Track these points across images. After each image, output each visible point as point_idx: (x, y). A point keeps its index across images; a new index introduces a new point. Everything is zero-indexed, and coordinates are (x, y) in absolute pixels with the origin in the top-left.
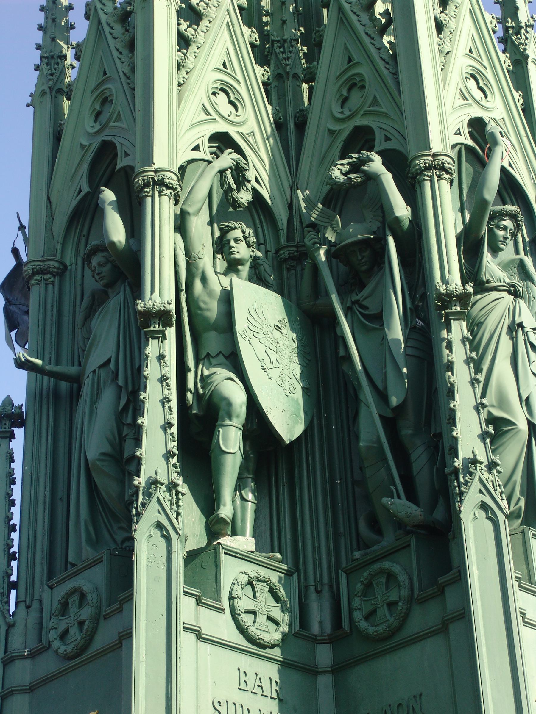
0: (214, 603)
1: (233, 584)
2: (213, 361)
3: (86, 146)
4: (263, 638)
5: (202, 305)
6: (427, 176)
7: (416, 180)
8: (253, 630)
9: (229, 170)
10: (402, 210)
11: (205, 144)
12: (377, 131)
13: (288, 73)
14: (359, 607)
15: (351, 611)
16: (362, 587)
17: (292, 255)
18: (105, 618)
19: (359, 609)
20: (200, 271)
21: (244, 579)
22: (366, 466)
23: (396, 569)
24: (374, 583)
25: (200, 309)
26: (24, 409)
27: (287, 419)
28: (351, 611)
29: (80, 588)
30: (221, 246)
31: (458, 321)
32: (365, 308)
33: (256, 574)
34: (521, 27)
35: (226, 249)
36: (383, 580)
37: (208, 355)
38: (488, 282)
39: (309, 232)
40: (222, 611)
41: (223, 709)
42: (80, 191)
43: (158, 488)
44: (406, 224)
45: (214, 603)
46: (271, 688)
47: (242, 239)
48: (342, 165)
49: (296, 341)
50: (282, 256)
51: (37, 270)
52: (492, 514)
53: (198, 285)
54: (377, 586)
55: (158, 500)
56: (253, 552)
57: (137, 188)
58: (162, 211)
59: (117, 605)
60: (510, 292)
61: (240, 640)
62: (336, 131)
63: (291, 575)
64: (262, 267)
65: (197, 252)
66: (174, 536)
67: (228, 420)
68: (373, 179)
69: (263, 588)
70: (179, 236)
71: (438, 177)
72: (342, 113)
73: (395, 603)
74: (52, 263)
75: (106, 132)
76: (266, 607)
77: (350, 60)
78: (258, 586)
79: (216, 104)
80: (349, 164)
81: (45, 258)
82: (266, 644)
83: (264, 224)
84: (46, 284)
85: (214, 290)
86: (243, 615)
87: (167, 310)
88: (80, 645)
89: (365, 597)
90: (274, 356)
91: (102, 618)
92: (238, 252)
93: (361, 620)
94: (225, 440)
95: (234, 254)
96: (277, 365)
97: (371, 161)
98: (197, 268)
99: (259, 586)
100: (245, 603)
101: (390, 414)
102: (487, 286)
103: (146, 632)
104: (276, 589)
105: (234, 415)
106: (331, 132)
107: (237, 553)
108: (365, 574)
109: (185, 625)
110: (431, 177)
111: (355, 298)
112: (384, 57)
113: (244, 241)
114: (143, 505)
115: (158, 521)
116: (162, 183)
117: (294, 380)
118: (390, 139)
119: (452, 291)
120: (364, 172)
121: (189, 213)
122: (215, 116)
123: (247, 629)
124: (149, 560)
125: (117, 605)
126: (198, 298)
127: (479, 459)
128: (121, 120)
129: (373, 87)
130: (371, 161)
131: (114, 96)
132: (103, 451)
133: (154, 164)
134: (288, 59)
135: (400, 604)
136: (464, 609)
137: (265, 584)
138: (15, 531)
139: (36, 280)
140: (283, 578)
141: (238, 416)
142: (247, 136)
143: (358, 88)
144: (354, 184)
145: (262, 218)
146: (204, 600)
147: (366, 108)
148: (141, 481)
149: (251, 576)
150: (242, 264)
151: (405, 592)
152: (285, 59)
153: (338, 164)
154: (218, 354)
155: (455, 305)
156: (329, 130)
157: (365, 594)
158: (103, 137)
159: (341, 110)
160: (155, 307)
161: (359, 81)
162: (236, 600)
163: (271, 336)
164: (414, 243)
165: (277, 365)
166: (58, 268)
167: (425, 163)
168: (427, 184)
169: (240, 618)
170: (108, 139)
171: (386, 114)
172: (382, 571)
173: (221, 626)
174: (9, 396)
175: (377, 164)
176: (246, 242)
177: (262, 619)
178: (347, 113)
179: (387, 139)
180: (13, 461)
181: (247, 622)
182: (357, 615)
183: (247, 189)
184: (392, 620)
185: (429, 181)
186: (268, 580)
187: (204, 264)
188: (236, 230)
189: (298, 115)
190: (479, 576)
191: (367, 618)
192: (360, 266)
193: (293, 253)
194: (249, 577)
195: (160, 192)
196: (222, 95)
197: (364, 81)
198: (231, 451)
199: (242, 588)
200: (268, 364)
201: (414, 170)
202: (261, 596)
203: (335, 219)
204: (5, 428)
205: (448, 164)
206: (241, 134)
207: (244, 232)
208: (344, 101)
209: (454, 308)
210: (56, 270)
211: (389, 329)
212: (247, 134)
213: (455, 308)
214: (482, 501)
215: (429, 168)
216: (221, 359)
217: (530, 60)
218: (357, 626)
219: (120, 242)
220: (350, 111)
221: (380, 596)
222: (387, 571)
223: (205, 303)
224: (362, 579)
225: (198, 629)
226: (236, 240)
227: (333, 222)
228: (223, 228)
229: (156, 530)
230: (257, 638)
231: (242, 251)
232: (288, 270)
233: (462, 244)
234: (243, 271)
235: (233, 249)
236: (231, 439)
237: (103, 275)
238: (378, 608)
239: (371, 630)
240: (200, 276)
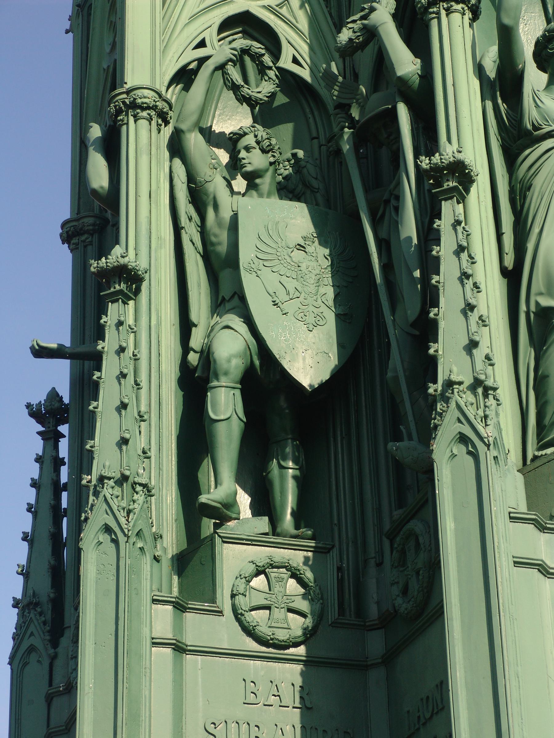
0: (206, 606)
4: (277, 637)
5: (213, 239)
6: (433, 13)
8: (264, 630)
9: (230, 63)
14: (396, 581)
20: (211, 197)
27: (310, 360)
31: (450, 201)
37: (223, 299)
38: (536, 128)
41: (219, 731)
43: (106, 484)
44: (416, 80)
45: (206, 606)
46: (291, 696)
47: (255, 145)
48: (354, 21)
49: (328, 257)
51: (73, 233)
52: (472, 447)
56: (266, 534)
61: (252, 645)
64: (305, 170)
65: (202, 175)
66: (122, 539)
67: (216, 381)
70: (177, 162)
74: (86, 220)
78: (273, 575)
81: (82, 214)
82: (283, 643)
83: (316, 113)
84: (85, 247)
87: (121, 265)
90: (291, 285)
92: (250, 163)
93: (398, 596)
94: (213, 407)
95: (245, 167)
96: (297, 294)
98: (206, 194)
102: (536, 136)
103: (95, 658)
104: (301, 574)
105: (220, 373)
107: (243, 539)
109: (154, 641)
110: (438, 13)
113: (258, 147)
116: (134, 105)
117: (324, 308)
119: (437, 164)
121: (182, 131)
123: (254, 630)
124: (99, 572)
126: (210, 231)
127: (453, 380)
133: (126, 83)
137: (284, 570)
139: (73, 244)
140: (311, 558)
141: (226, 374)
142: (277, 8)
144: (357, 45)
149: (259, 564)
150: (260, 176)
153: (348, 23)
154: (232, 297)
155: (448, 180)
162: (237, 597)
163: (289, 260)
165: (297, 294)
166: (94, 225)
169: (243, 618)
173: (221, 631)
174: (54, 388)
176: (260, 148)
181: (253, 622)
183: (270, 78)
185: (436, 20)
186: (287, 564)
187: (215, 187)
188: (247, 136)
190: (457, 530)
195: (135, 116)
198: (222, 417)
203: (359, 92)
204: (49, 427)
207: (256, 136)
210: (91, 228)
211: (401, 225)
212: (277, 6)
213: (447, 184)
214: (460, 433)
219: (102, 187)
223: (216, 236)
226: (248, 149)
227: (358, 97)
228: (232, 137)
229: (106, 534)
230: (269, 638)
233: (498, 88)
234: (263, 184)
235: (244, 161)
240: (212, 203)
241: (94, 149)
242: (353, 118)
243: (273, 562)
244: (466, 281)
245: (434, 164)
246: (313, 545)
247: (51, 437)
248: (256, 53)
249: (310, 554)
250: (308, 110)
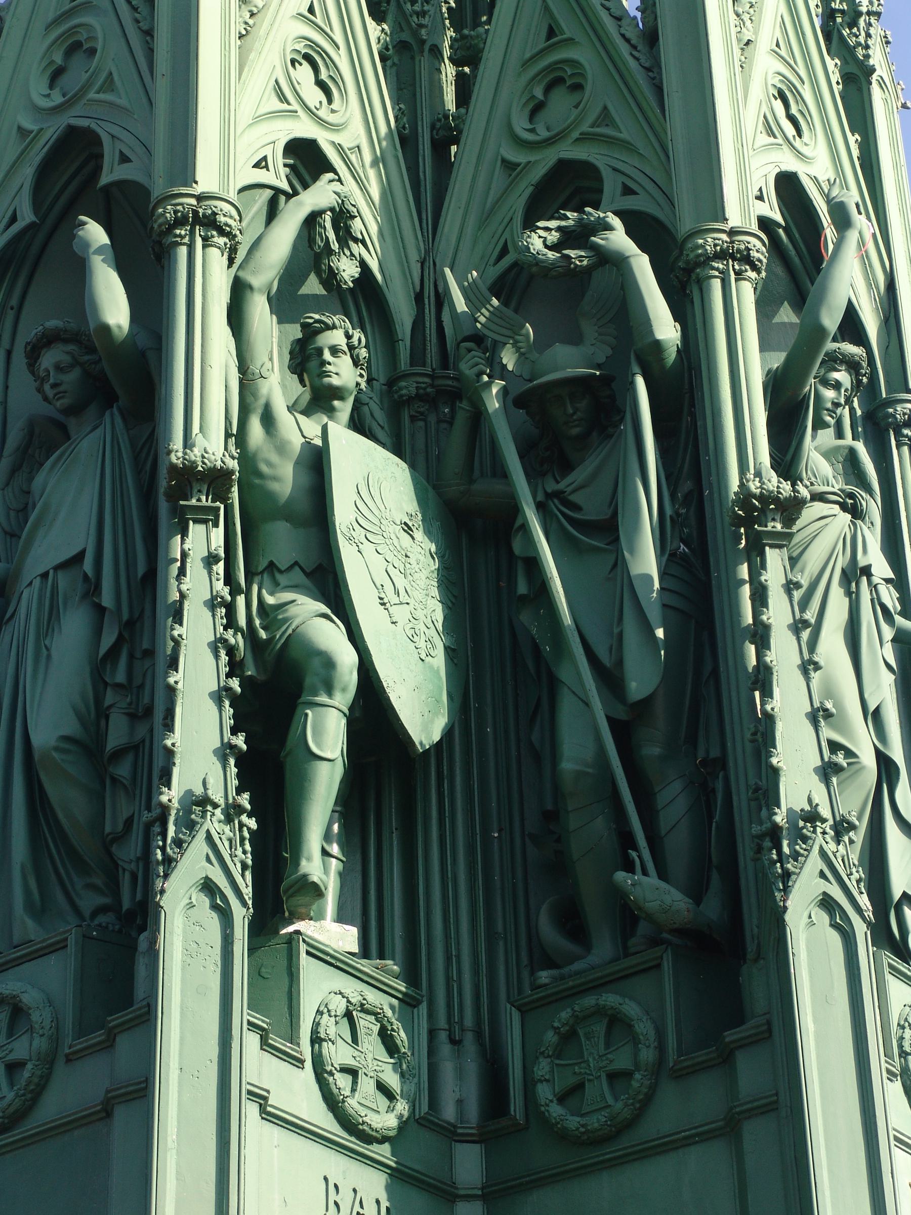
1: (319, 1012)
2: (282, 579)
3: (32, 132)
4: (369, 1122)
5: (264, 468)
6: (717, 269)
7: (693, 276)
8: (352, 1104)
9: (329, 213)
10: (666, 329)
11: (278, 160)
12: (606, 173)
13: (423, 42)
14: (547, 1077)
15: (529, 1084)
16: (555, 1039)
17: (421, 391)
18: (68, 1060)
19: (547, 1081)
20: (262, 401)
21: (339, 1005)
22: (570, 809)
23: (631, 1009)
24: (581, 1033)
25: (260, 475)
28: (529, 1084)
29: (14, 997)
30: (304, 359)
32: (576, 507)
33: (360, 998)
34: (860, 14)
35: (313, 364)
36: (600, 1029)
37: (271, 565)
39: (470, 351)
40: (299, 1062)
42: (13, 219)
43: (209, 814)
44: (671, 355)
45: (287, 1047)
47: (345, 348)
48: (547, 229)
50: (404, 392)
52: (841, 919)
53: (256, 429)
54: (588, 1039)
55: (209, 838)
57: (160, 226)
58: (208, 276)
59: (100, 1036)
60: (844, 507)
62: (518, 165)
63: (415, 1007)
64: (365, 409)
67: (325, 695)
68: (615, 263)
69: (371, 1026)
71: (736, 273)
72: (532, 131)
73: (627, 1075)
75: (77, 110)
76: (376, 1063)
77: (551, 33)
78: (362, 1022)
79: (299, 83)
80: (559, 229)
82: (374, 1134)
85: (289, 442)
86: (338, 1075)
87: (228, 469)
88: (11, 1110)
89: (558, 1058)
90: (400, 582)
91: (61, 1060)
92: (337, 374)
93: (551, 1101)
94: (317, 733)
95: (330, 376)
97: (609, 228)
98: (255, 395)
99: (366, 1023)
100: (339, 1053)
101: (621, 714)
103: (179, 1092)
104: (393, 1030)
105: (338, 685)
106: (509, 166)
107: (327, 954)
108: (565, 1015)
111: (551, 486)
112: (628, 35)
113: (348, 354)
114: (178, 843)
115: (207, 878)
116: (211, 222)
118: (633, 192)
120: (595, 248)
121: (251, 288)
122: (295, 106)
123: (344, 1101)
125: (100, 1036)
128: (113, 90)
129: (599, 90)
130: (609, 228)
131: (100, 40)
132: (67, 731)
134: (423, 14)
135: (637, 1076)
136: (777, 1094)
137: (372, 1018)
141: (344, 690)
142: (348, 152)
143: (568, 87)
145: (365, 314)
146: (272, 1039)
147: (585, 128)
148: (172, 796)
149: (353, 1000)
150: (342, 398)
151: (647, 1055)
152: (418, 14)
154: (291, 567)
155: (774, 520)
156: (504, 161)
157: (559, 1053)
158: (74, 118)
160: (206, 461)
161: (573, 75)
162: (325, 1044)
164: (685, 394)
167: (715, 245)
168: (716, 284)
169: (331, 1079)
170: (84, 123)
171: (628, 143)
172: (599, 1012)
173: (297, 1092)
175: (618, 238)
176: (352, 356)
177: (367, 1086)
178: (544, 134)
181: (344, 1089)
182: (544, 1092)
183: (352, 255)
184: (620, 1105)
185: (719, 280)
186: (379, 1011)
187: (270, 390)
188: (334, 331)
189: (438, 125)
190: (816, 1032)
191: (562, 1099)
192: (571, 426)
193: (425, 389)
194: (349, 1001)
195: (205, 239)
196: (306, 68)
197: (582, 75)
199: (337, 1023)
200: (391, 597)
201: (692, 256)
202: (366, 1041)
203: (524, 332)
205: (758, 251)
206: (339, 148)
207: (348, 337)
208: (537, 109)
209: (770, 524)
212: (349, 149)
213: (772, 524)
214: (825, 893)
215: (722, 255)
216: (297, 576)
217: (875, 77)
218: (543, 1113)
219: (120, 327)
220: (548, 129)
221: (594, 1059)
222: (609, 1012)
223: (269, 464)
224: (556, 1024)
225: (265, 1094)
226: (334, 351)
231: (344, 373)
232: (413, 419)
235: (329, 368)
236: (327, 732)
237: (61, 389)
238: (589, 1080)
239: (573, 1122)
240: (260, 411)
241: (103, 260)
242: (504, 367)
243: (365, 1002)
244: (812, 674)
245: (768, 491)
246: (404, 989)
248: (348, 211)
249: (395, 1002)
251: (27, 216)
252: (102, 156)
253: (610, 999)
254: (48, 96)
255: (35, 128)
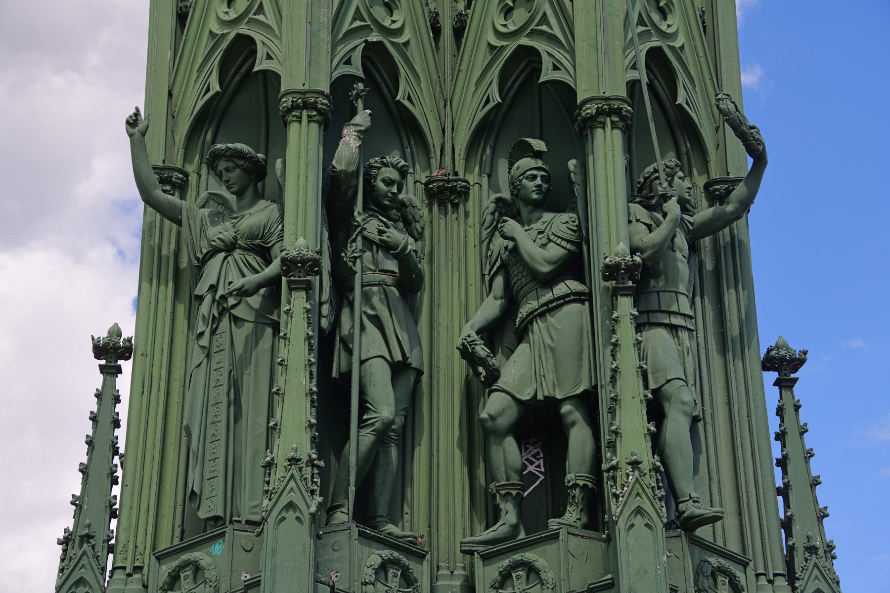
12: (545, 58)
24: (514, 575)
26: (133, 341)
62: (496, 47)
72: (505, 26)
106: (491, 47)
110: (604, 124)
138: (117, 484)
159: (504, 23)
178: (512, 28)
179: (555, 68)
180: (119, 401)
247: (111, 371)
250: (406, 144)
251: (216, 87)
252: (256, 52)
253: (529, 555)
254: (227, 13)
255: (220, 33)
